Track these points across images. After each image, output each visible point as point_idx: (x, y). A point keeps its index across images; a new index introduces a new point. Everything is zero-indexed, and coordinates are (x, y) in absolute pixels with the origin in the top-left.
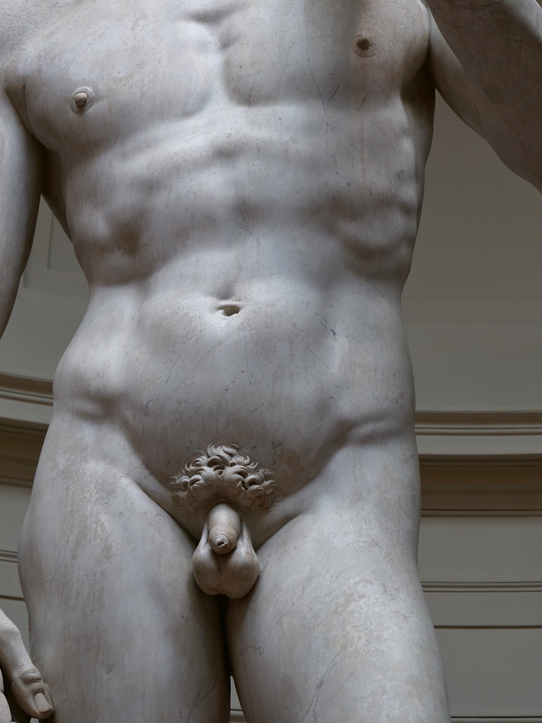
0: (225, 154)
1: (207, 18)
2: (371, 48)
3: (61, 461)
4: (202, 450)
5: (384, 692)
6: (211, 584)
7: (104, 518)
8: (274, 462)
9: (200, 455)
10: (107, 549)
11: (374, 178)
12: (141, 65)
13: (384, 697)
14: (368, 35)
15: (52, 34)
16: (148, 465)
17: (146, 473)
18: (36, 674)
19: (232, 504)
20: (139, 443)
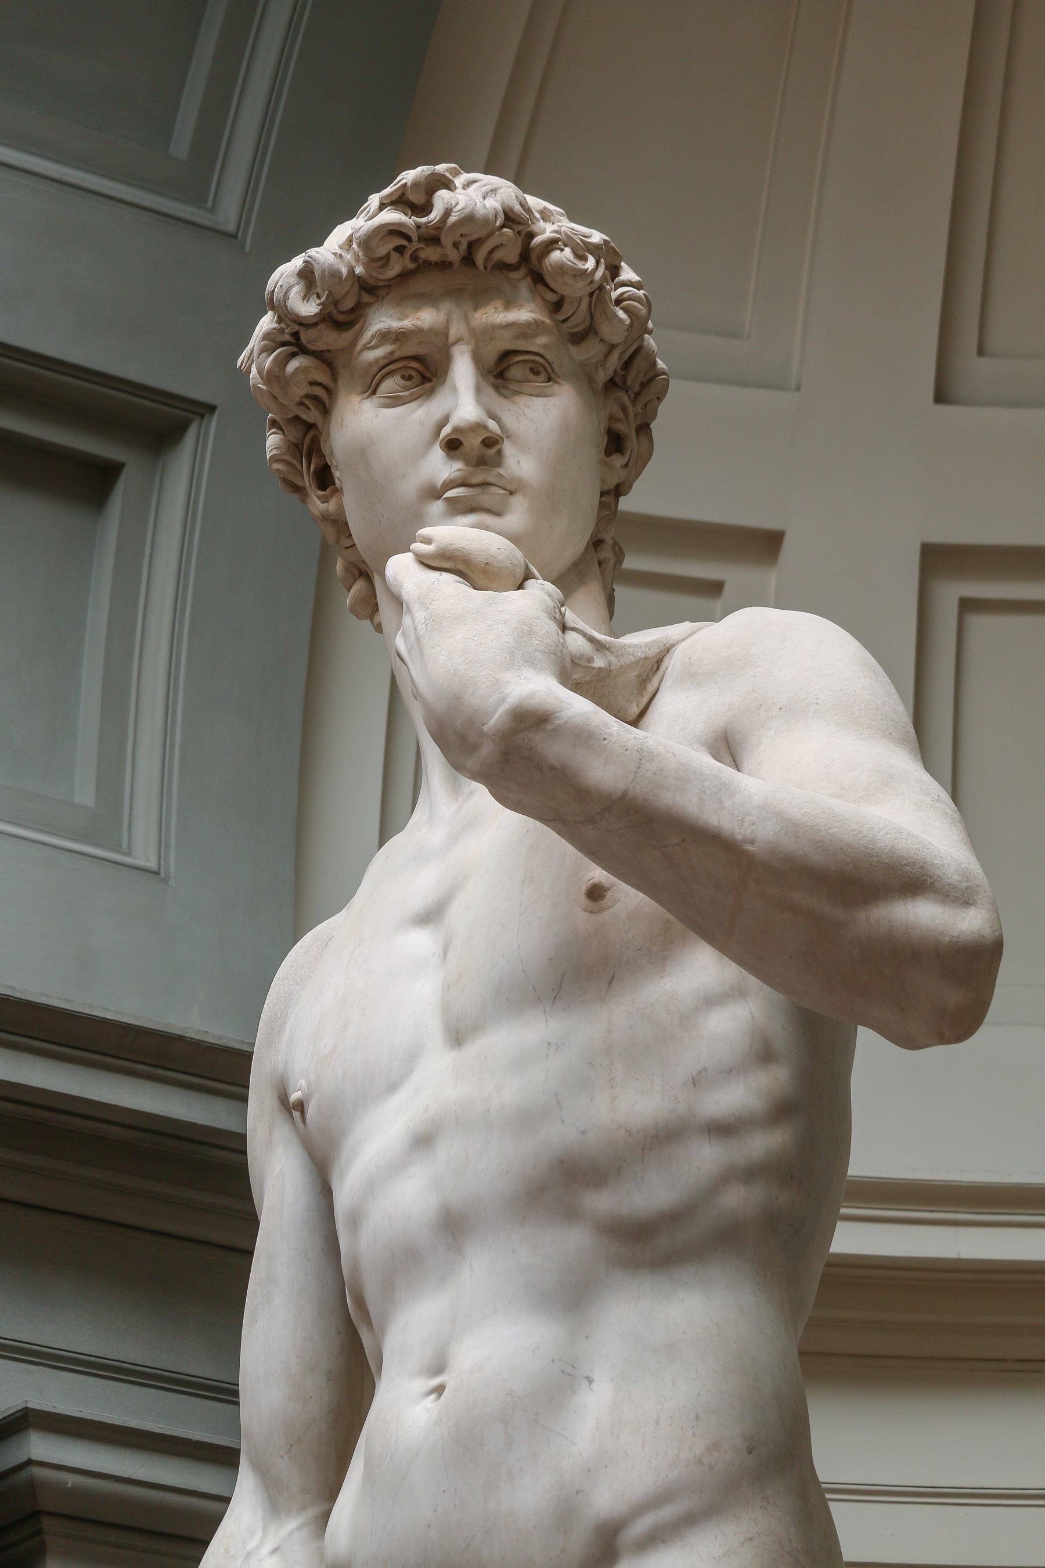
0: (423, 1141)
2: (609, 895)
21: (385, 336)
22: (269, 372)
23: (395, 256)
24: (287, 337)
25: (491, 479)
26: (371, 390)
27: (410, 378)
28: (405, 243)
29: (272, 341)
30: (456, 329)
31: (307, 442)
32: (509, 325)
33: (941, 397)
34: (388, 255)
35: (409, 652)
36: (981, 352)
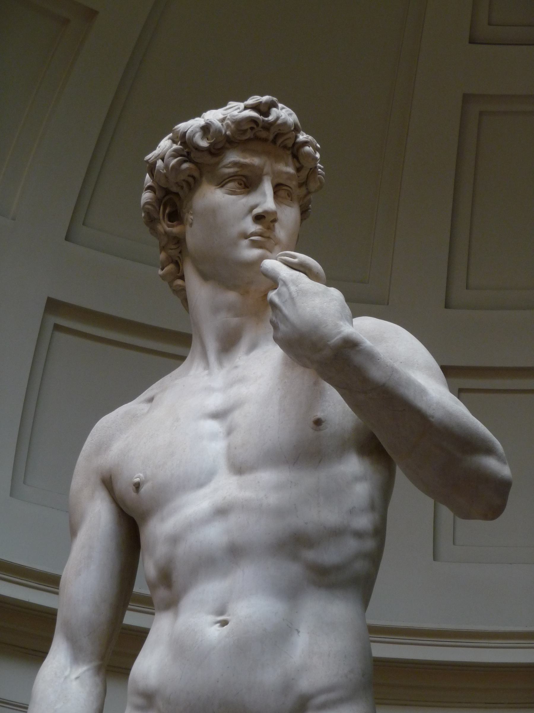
0: (221, 512)
2: (324, 424)
11: (329, 516)
14: (322, 414)
21: (236, 164)
22: (173, 166)
23: (249, 131)
24: (185, 153)
25: (271, 236)
26: (221, 184)
27: (241, 184)
28: (255, 126)
29: (176, 154)
30: (267, 169)
31: (166, 199)
32: (287, 173)
33: (67, 239)
34: (247, 129)
36: (84, 224)
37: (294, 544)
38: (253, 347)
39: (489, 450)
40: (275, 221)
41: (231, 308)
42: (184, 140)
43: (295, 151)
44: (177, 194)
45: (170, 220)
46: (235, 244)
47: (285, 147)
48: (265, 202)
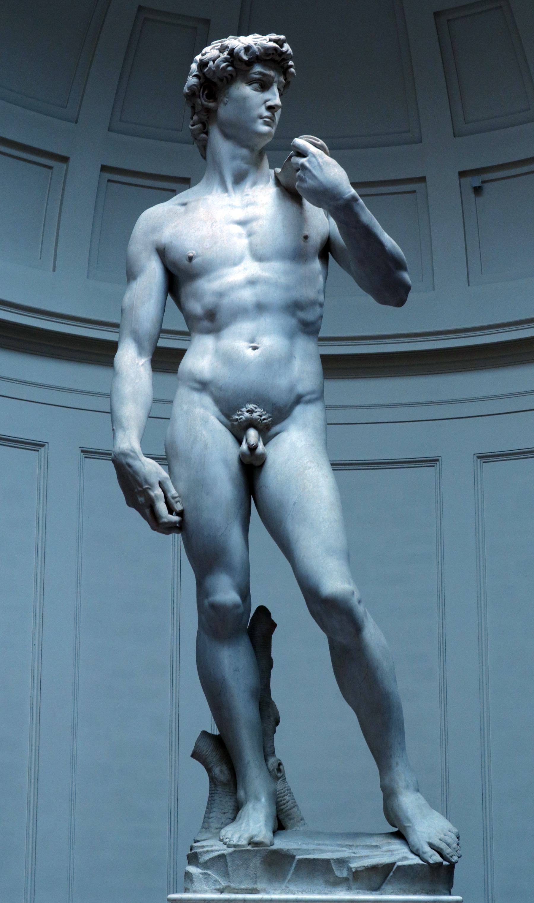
0: (252, 282)
1: (242, 223)
3: (185, 407)
4: (244, 405)
5: (321, 508)
6: (247, 460)
7: (204, 432)
8: (272, 411)
9: (243, 407)
10: (206, 445)
11: (310, 293)
12: (215, 243)
13: (321, 510)
15: (176, 226)
16: (222, 411)
17: (220, 414)
18: (177, 495)
19: (256, 428)
20: (218, 401)
21: (260, 73)
22: (223, 67)
29: (225, 60)
30: (276, 79)
35: (314, 167)
37: (294, 307)
38: (254, 184)
39: (405, 269)
40: (276, 111)
41: (243, 158)
42: (232, 52)
43: (284, 71)
44: (215, 84)
45: (207, 98)
46: (254, 121)
47: (282, 67)
48: (275, 99)
